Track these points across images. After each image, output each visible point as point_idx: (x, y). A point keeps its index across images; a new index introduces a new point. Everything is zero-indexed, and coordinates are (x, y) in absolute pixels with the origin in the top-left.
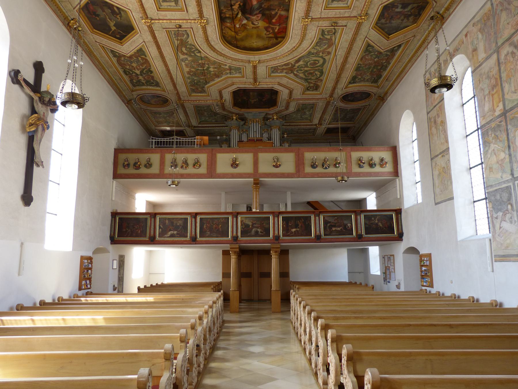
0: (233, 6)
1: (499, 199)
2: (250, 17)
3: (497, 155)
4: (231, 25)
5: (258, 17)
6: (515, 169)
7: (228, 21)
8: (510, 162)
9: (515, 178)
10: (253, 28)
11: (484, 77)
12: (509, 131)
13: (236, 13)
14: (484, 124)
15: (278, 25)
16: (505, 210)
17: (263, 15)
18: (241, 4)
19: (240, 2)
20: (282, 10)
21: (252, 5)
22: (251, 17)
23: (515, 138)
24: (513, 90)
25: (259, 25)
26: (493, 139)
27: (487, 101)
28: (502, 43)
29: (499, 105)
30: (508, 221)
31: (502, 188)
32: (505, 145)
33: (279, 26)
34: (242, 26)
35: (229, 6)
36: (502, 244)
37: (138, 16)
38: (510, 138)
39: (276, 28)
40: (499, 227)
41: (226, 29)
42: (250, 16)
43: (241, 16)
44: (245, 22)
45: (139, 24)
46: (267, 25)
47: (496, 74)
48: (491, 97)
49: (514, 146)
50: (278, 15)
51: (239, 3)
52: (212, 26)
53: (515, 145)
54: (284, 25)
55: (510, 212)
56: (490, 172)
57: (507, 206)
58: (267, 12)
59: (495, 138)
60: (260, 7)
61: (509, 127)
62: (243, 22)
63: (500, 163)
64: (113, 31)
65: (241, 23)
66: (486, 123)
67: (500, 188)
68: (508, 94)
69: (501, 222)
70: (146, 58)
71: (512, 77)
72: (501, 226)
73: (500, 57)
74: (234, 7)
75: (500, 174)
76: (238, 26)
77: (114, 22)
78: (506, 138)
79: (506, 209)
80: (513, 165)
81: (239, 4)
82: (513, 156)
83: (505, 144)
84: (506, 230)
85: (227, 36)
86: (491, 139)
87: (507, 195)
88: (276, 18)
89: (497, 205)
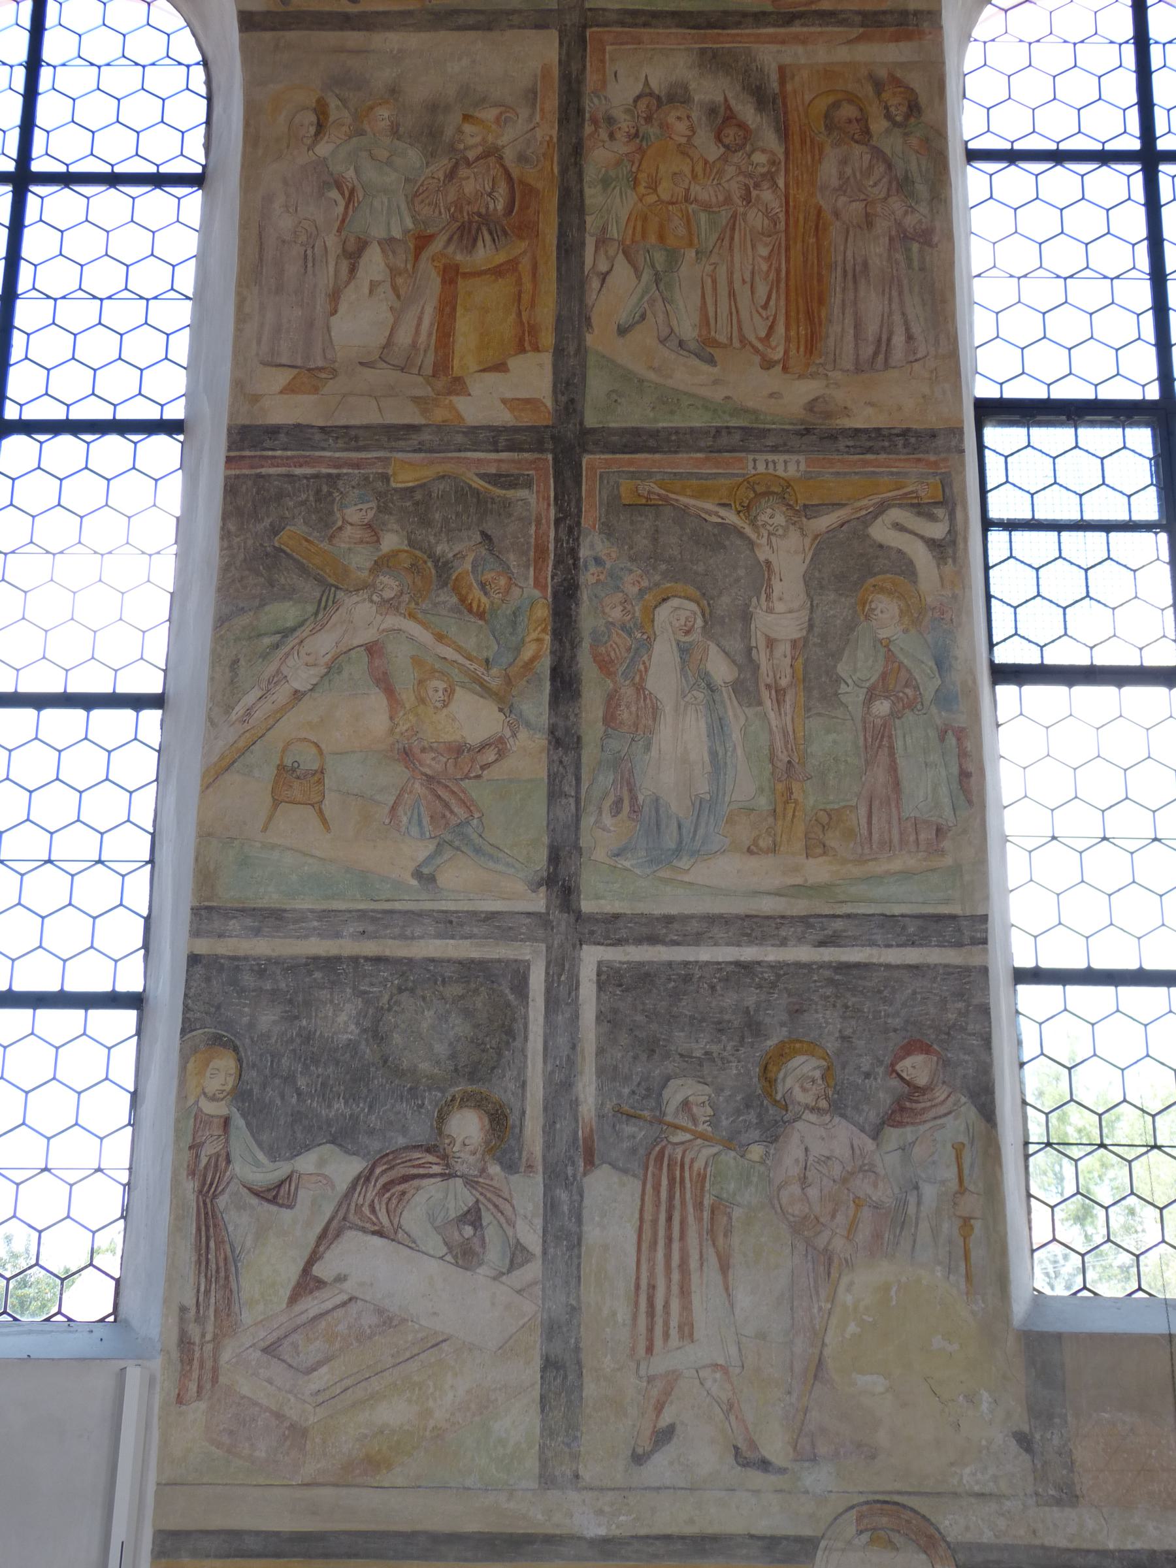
1: (352, 1046)
3: (408, 697)
6: (600, 855)
8: (554, 794)
9: (579, 916)
11: (384, 113)
12: (588, 577)
14: (298, 426)
16: (401, 1141)
23: (648, 644)
24: (688, 329)
26: (382, 564)
27: (373, 286)
28: (634, 13)
29: (512, 363)
30: (435, 1244)
31: (410, 962)
32: (527, 653)
36: (297, 1434)
38: (587, 621)
40: (290, 1272)
47: (522, 158)
48: (434, 284)
49: (628, 692)
53: (640, 688)
55: (461, 1168)
56: (276, 803)
57: (442, 1118)
59: (414, 568)
61: (592, 545)
63: (431, 763)
66: (322, 429)
67: (377, 960)
68: (623, 331)
69: (327, 1237)
71: (691, 254)
72: (318, 1270)
73: (591, 79)
75: (423, 851)
78: (543, 612)
79: (420, 1131)
80: (587, 821)
82: (589, 753)
83: (518, 650)
84: (380, 1311)
86: (360, 561)
87: (459, 1027)
89: (302, 1082)
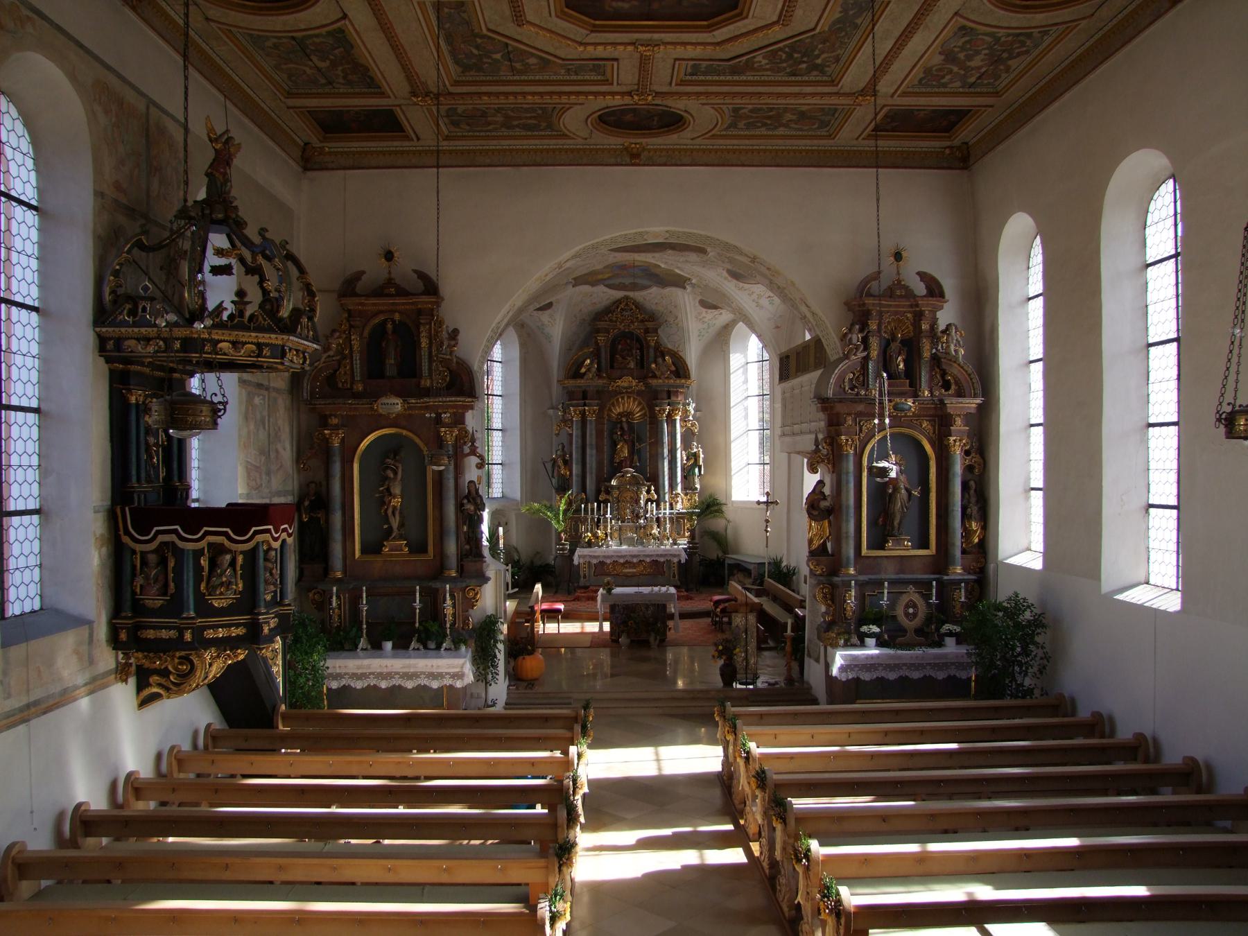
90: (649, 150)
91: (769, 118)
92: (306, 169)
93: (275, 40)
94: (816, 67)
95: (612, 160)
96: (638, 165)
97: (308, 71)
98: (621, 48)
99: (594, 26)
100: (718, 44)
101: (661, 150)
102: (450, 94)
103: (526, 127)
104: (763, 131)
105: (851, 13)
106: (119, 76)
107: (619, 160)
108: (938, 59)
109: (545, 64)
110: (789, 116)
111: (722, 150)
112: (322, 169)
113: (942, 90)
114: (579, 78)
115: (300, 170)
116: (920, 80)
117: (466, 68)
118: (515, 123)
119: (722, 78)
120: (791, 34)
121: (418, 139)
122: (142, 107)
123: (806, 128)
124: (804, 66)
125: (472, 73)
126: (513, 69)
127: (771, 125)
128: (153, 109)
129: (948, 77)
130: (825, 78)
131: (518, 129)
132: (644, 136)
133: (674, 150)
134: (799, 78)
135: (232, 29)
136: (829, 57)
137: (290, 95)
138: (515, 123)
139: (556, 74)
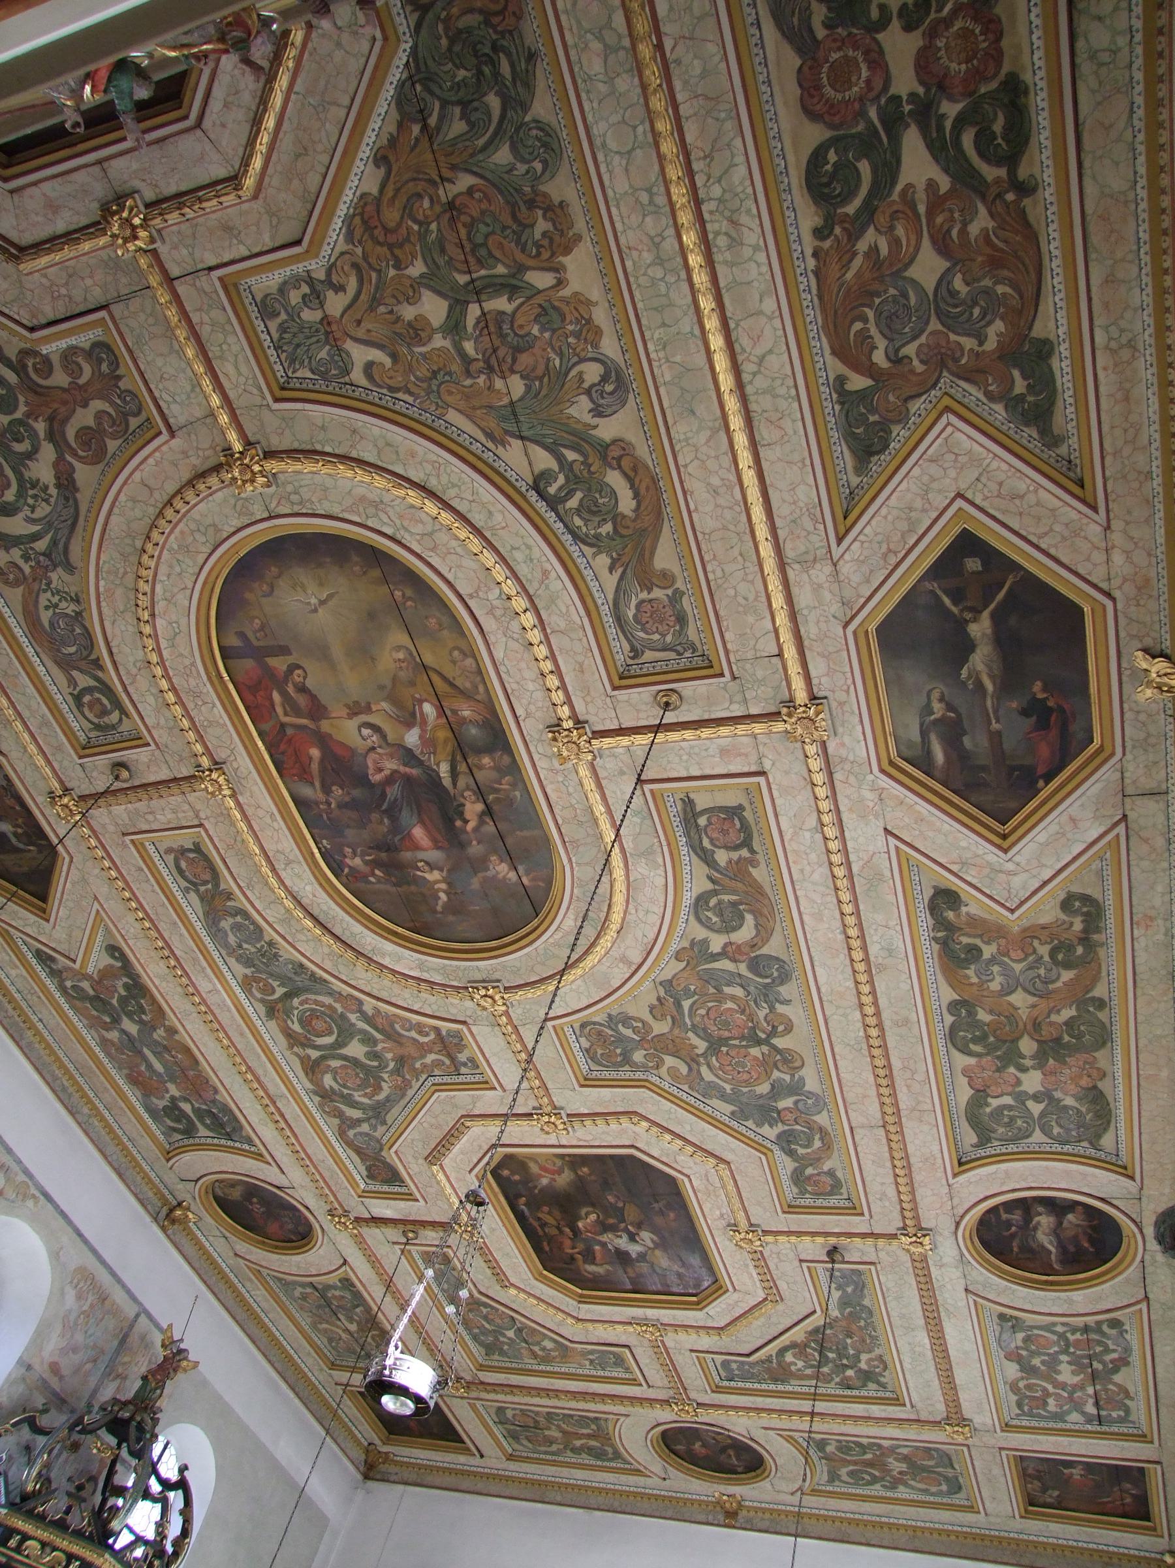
0: (483, 814)
2: (405, 765)
4: (455, 712)
5: (380, 770)
7: (474, 731)
10: (368, 709)
13: (461, 783)
15: (290, 731)
17: (362, 780)
18: (458, 823)
19: (466, 832)
20: (317, 803)
21: (422, 822)
22: (402, 769)
25: (352, 725)
33: (283, 726)
34: (413, 714)
35: (495, 808)
37: (846, 739)
39: (286, 714)
41: (468, 685)
42: (408, 770)
43: (438, 765)
44: (412, 738)
45: (848, 692)
46: (325, 726)
50: (317, 784)
51: (470, 826)
52: (528, 715)
54: (266, 727)
58: (357, 793)
60: (392, 813)
62: (421, 737)
64: (986, 606)
65: (423, 731)
70: (842, 369)
74: (480, 807)
76: (428, 708)
77: (964, 673)
81: (466, 822)
85: (445, 633)
88: (315, 766)
90: (749, 1509)
91: (871, 1464)
92: (366, 1477)
93: (300, 1289)
94: (867, 1377)
95: (702, 1518)
96: (734, 1527)
97: (344, 1336)
98: (619, 1328)
99: (541, 1274)
100: (722, 1329)
101: (764, 1510)
102: (482, 1383)
103: (590, 1451)
104: (877, 1490)
105: (849, 1290)
106: (113, 1274)
107: (710, 1518)
108: (1012, 1370)
109: (564, 1350)
110: (897, 1466)
111: (842, 1520)
112: (383, 1480)
113: (1060, 1425)
114: (607, 1374)
115: (359, 1477)
116: (1019, 1405)
117: (490, 1349)
118: (578, 1443)
119: (764, 1386)
120: (796, 1319)
121: (482, 1456)
122: (130, 1310)
123: (934, 1489)
124: (850, 1373)
125: (496, 1357)
126: (534, 1355)
127: (883, 1479)
128: (143, 1319)
129: (1051, 1401)
130: (888, 1394)
131: (584, 1455)
132: (728, 1481)
133: (779, 1512)
134: (855, 1393)
135: (265, 1272)
136: (871, 1360)
137: (333, 1366)
138: (578, 1443)
139: (582, 1366)
